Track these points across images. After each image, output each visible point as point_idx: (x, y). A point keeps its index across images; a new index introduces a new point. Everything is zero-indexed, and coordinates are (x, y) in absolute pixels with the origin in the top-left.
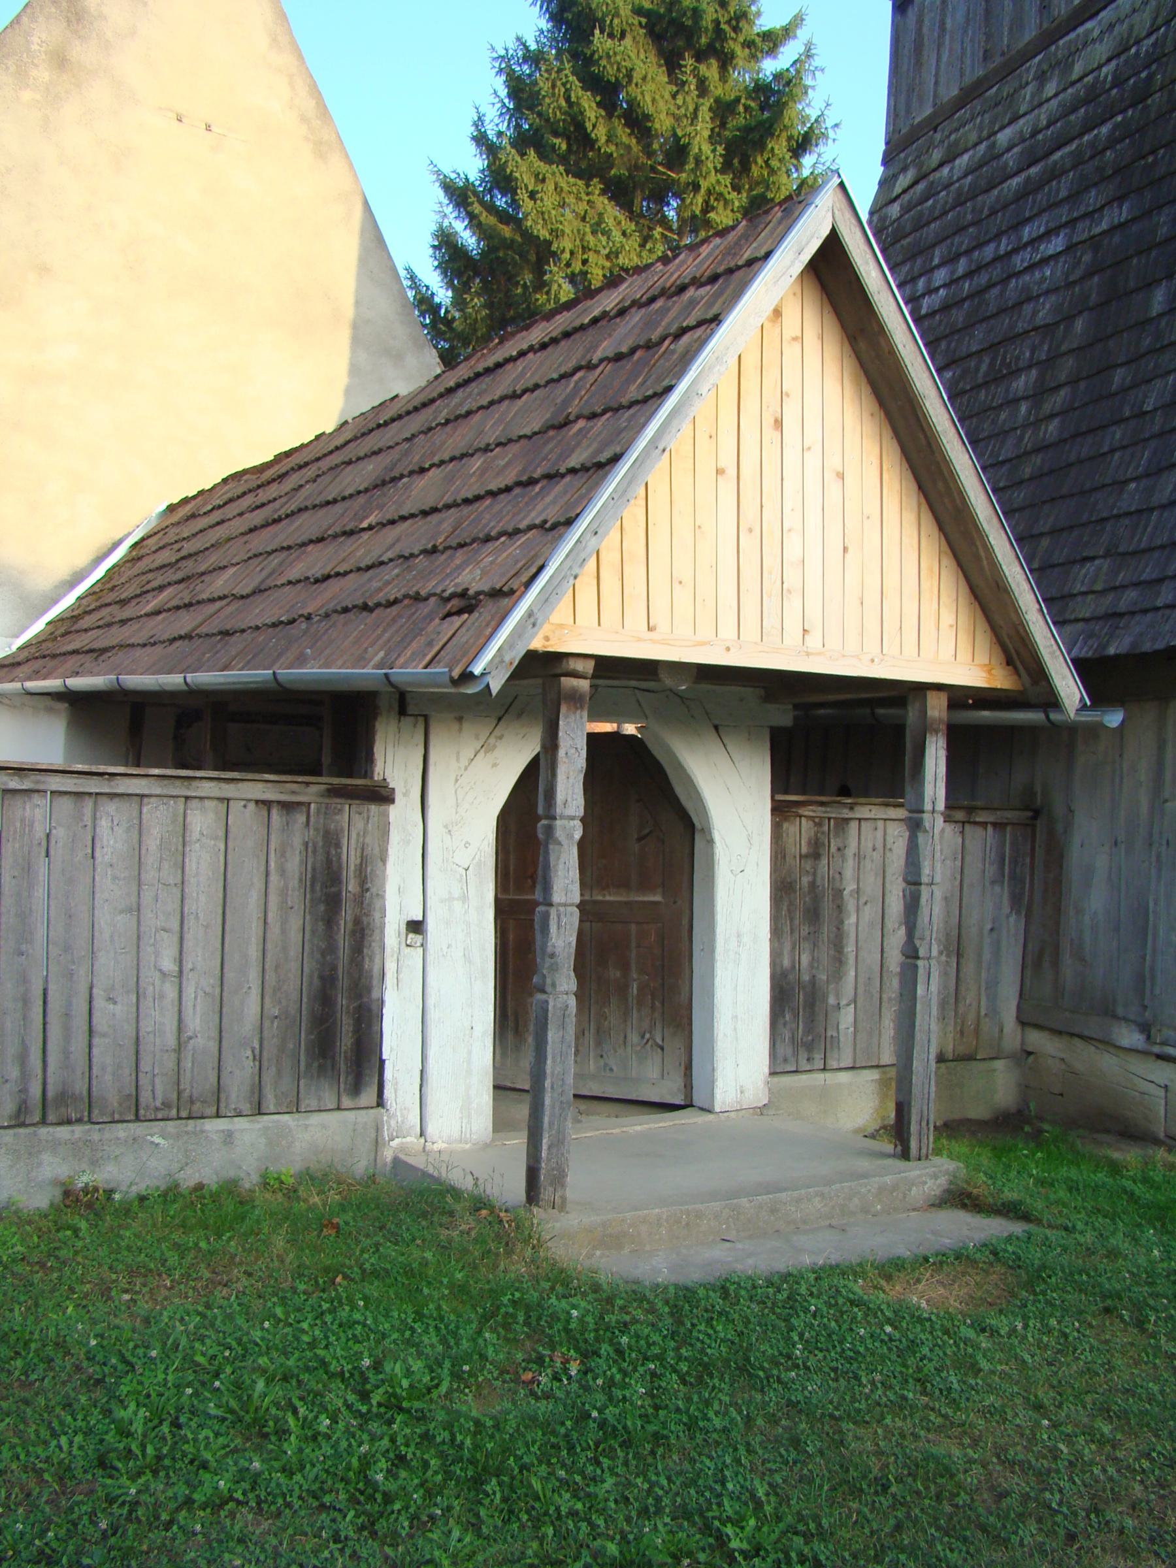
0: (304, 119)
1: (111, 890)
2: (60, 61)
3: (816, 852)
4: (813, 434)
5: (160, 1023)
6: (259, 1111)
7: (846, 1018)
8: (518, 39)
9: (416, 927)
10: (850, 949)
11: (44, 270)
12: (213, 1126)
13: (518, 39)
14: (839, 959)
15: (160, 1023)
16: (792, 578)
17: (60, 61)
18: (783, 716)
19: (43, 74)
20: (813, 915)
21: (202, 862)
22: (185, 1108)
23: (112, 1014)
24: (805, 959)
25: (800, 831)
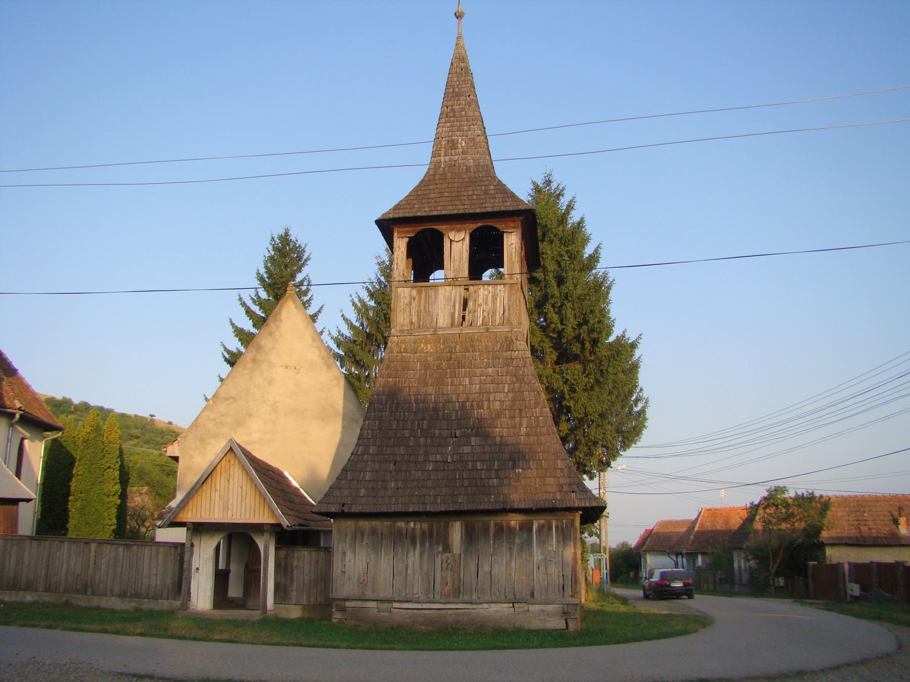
0: (323, 359)
1: (147, 561)
2: (254, 361)
3: (286, 557)
4: (236, 480)
5: (153, 583)
6: (168, 599)
7: (294, 593)
8: (582, 219)
9: (198, 569)
10: (295, 578)
11: (250, 415)
12: (160, 601)
13: (582, 219)
14: (292, 580)
15: (153, 583)
16: (230, 506)
17: (254, 361)
18: (279, 530)
19: (250, 365)
20: (286, 570)
21: (161, 557)
22: (157, 597)
23: (145, 581)
24: (283, 580)
25: (283, 553)
